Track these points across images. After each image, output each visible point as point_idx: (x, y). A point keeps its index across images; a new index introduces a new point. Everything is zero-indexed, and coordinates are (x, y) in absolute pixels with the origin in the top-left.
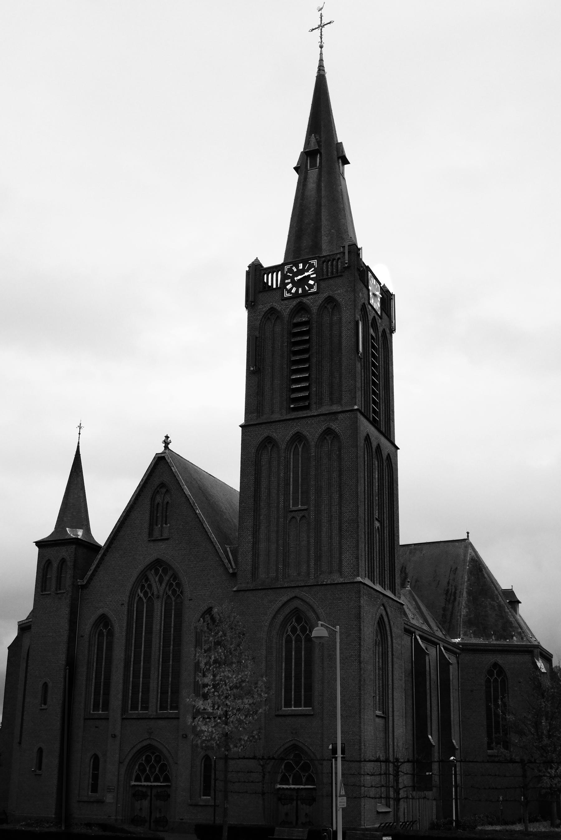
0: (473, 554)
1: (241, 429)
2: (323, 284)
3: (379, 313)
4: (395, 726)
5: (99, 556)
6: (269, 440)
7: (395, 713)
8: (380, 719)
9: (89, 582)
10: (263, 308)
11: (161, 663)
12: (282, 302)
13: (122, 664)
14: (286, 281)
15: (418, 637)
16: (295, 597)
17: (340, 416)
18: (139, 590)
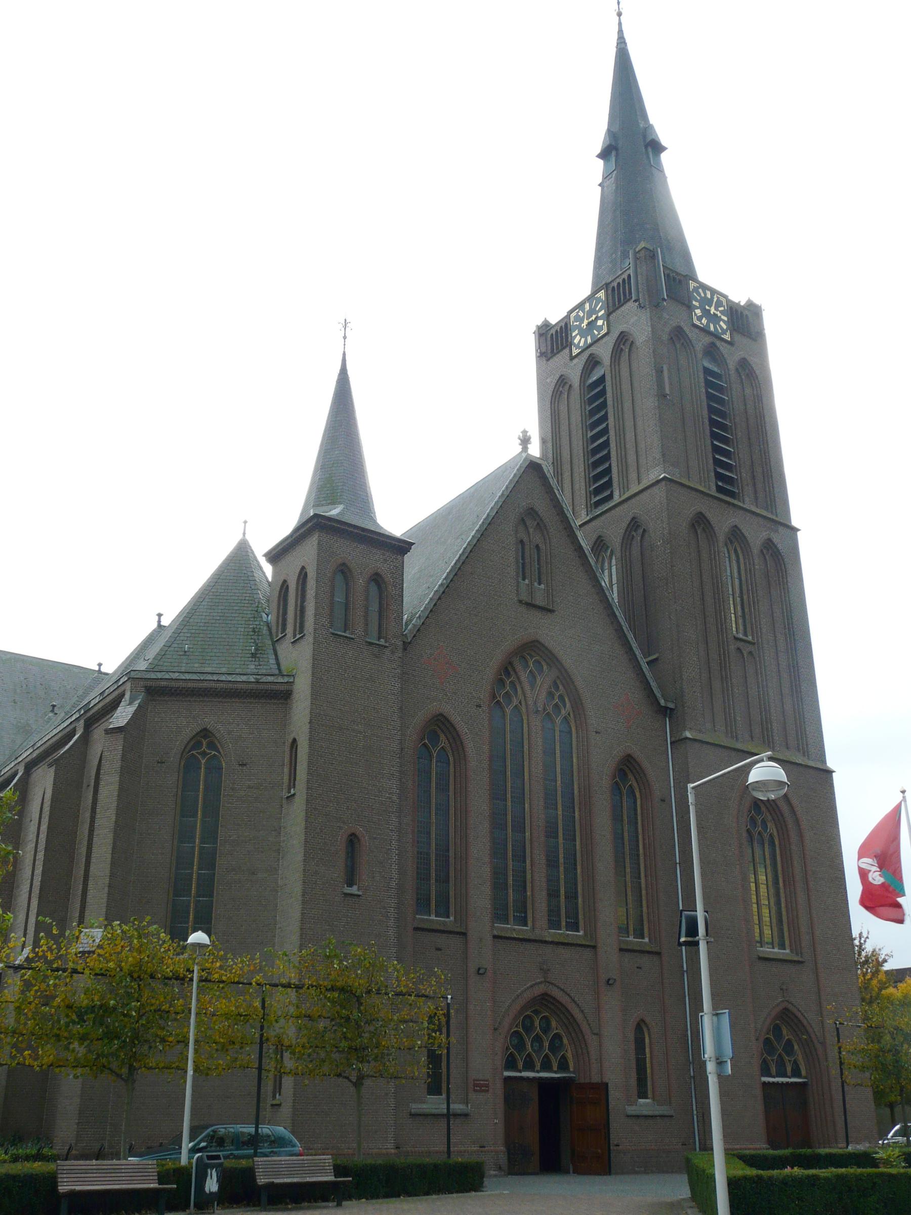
3: (727, 337)
10: (552, 380)
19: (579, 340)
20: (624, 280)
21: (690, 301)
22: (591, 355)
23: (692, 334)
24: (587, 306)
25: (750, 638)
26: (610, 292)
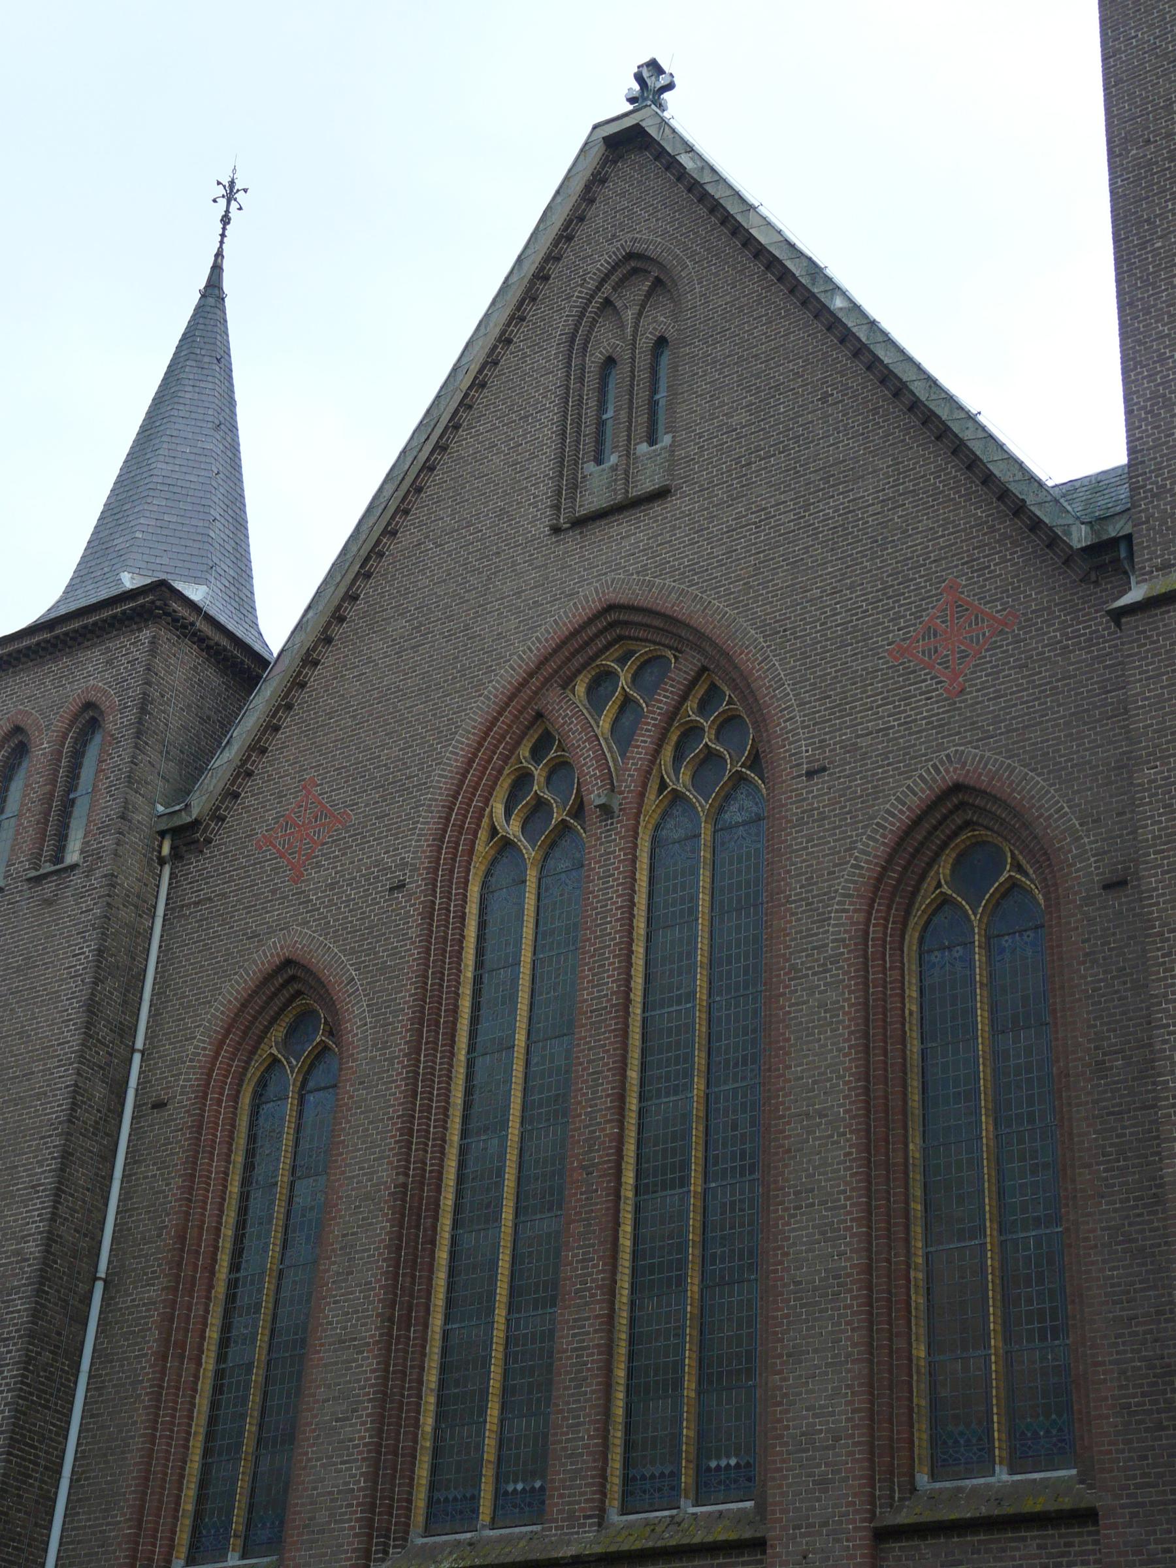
11: (628, 1192)
13: (382, 1227)
18: (499, 809)
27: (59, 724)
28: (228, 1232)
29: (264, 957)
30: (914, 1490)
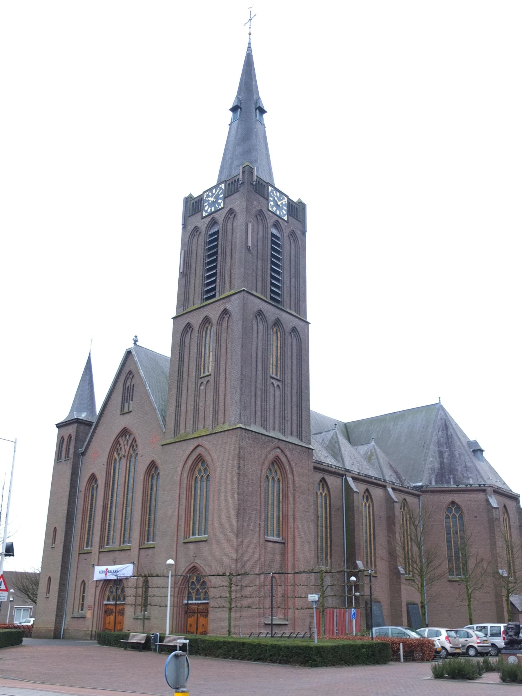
0: (443, 414)
1: (172, 320)
2: (226, 199)
3: (285, 218)
4: (296, 550)
5: (92, 430)
6: (189, 325)
7: (297, 539)
8: (277, 544)
9: (86, 451)
10: (190, 228)
12: (202, 221)
14: (205, 205)
15: (350, 480)
16: (199, 445)
17: (233, 298)
19: (208, 209)
20: (235, 181)
21: (268, 197)
22: (213, 218)
23: (267, 214)
24: (214, 191)
25: (278, 378)
26: (227, 185)
27: (67, 437)
28: (89, 508)
29: (90, 473)
30: (144, 543)
